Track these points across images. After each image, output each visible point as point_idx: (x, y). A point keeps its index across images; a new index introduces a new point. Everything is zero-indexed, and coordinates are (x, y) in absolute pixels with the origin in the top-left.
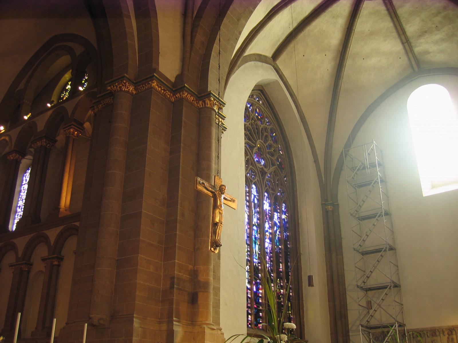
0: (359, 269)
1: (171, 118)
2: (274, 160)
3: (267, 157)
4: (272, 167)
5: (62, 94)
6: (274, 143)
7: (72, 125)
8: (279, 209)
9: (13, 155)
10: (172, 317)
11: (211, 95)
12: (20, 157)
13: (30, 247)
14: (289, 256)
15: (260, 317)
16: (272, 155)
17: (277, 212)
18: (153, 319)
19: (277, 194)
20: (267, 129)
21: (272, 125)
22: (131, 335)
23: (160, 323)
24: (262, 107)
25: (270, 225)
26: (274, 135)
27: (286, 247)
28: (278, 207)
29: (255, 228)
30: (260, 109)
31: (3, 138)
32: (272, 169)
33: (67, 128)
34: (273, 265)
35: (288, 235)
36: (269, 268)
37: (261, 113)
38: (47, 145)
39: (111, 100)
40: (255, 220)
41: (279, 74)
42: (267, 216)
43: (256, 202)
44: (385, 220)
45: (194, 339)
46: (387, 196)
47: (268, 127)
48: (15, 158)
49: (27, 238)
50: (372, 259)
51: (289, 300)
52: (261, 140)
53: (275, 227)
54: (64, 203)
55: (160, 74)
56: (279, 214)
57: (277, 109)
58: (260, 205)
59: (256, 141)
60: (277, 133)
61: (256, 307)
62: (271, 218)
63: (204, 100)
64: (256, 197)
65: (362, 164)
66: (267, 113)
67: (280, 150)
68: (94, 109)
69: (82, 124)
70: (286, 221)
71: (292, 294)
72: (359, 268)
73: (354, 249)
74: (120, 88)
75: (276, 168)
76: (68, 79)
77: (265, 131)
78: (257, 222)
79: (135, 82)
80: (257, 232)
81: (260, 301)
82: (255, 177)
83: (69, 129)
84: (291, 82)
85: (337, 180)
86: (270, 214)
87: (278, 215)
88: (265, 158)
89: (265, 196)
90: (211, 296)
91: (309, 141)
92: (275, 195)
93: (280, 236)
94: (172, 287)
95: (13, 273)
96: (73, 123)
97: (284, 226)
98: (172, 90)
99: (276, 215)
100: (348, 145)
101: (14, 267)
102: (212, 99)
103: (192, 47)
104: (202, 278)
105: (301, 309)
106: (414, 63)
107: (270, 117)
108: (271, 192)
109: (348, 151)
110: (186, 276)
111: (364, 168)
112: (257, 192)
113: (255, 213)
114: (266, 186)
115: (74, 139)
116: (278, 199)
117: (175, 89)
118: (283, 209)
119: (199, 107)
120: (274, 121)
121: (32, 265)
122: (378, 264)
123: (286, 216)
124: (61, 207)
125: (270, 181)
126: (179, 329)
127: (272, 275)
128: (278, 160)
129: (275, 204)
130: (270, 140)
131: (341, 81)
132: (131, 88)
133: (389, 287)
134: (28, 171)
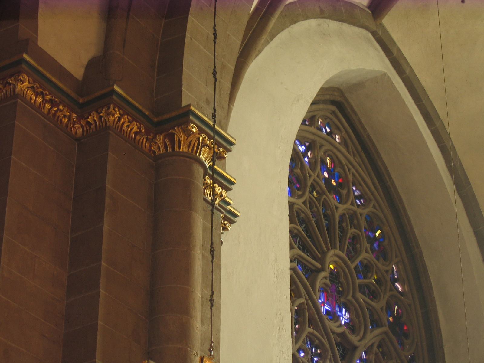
3: (357, 300)
4: (371, 332)
6: (378, 259)
11: (191, 118)
16: (373, 295)
21: (371, 205)
26: (377, 234)
37: (338, 169)
47: (359, 211)
52: (338, 252)
59: (324, 254)
67: (396, 280)
75: (386, 333)
77: (352, 223)
119: (154, 152)
128: (389, 309)
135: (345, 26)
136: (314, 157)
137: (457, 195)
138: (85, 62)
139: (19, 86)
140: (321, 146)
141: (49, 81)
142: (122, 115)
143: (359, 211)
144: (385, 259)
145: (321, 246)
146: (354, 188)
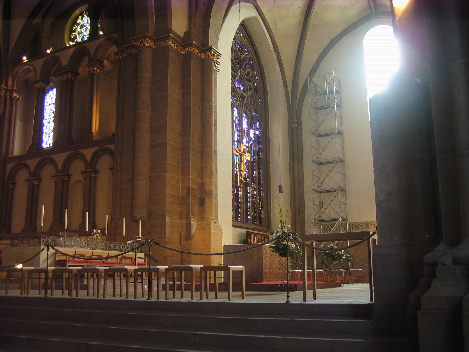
0: (316, 176)
1: (182, 68)
2: (251, 86)
3: (246, 83)
4: (249, 92)
5: (73, 27)
6: (251, 71)
7: (96, 64)
8: (254, 127)
9: (40, 84)
10: (189, 215)
11: (212, 49)
12: (46, 85)
13: (68, 162)
14: (261, 165)
15: (240, 213)
16: (250, 81)
17: (253, 129)
18: (177, 216)
19: (253, 115)
20: (246, 58)
21: (250, 54)
22: (165, 227)
23: (181, 219)
24: (243, 40)
25: (247, 140)
26: (251, 63)
27: (259, 157)
28: (253, 125)
29: (236, 143)
30: (241, 41)
31: (26, 67)
32: (250, 93)
33: (91, 66)
34: (249, 172)
35: (260, 148)
36: (246, 175)
37: (242, 45)
38: (72, 78)
39: (133, 51)
40: (236, 137)
41: (259, 11)
42: (245, 133)
43: (237, 122)
44: (338, 139)
45: (203, 229)
46: (341, 118)
47: (247, 57)
48: (42, 86)
49: (65, 155)
50: (325, 169)
51: (260, 199)
52: (241, 70)
53: (251, 142)
54: (95, 129)
55: (174, 33)
56: (254, 131)
57: (255, 40)
58: (240, 124)
59: (237, 71)
60: (254, 61)
61: (236, 205)
62: (248, 135)
63: (206, 52)
64: (237, 118)
65: (323, 91)
66: (247, 44)
67: (256, 76)
68: (118, 55)
69: (102, 62)
70: (259, 136)
71: (263, 195)
72: (315, 175)
73: (312, 161)
74: (144, 44)
75: (253, 92)
76: (78, 14)
77: (245, 60)
78: (238, 139)
79: (154, 39)
80: (237, 147)
81: (239, 200)
82: (236, 102)
83: (93, 67)
84: (267, 17)
85: (301, 101)
86: (247, 131)
87: (253, 131)
88: (244, 84)
89: (243, 116)
90: (214, 200)
91: (280, 68)
92: (252, 115)
93: (254, 149)
94: (188, 195)
95: (55, 182)
96: (96, 62)
97: (258, 140)
98: (182, 45)
99: (252, 132)
100: (312, 74)
101: (55, 177)
102: (213, 53)
103: (196, 7)
104: (207, 188)
105: (269, 206)
106: (372, 5)
107: (249, 48)
108: (248, 113)
109: (311, 79)
110: (197, 187)
111: (324, 94)
112: (238, 114)
113: (236, 131)
114: (245, 108)
115: (97, 75)
116: (254, 119)
117: (185, 44)
118: (257, 126)
119: (202, 58)
120: (252, 51)
121: (70, 176)
122: (330, 173)
123: (259, 132)
124: (93, 132)
125: (247, 104)
126: (194, 223)
127: (248, 180)
128: (254, 84)
129: (251, 123)
130: (249, 69)
131: (310, 18)
132: (152, 44)
133: (337, 191)
134: (47, 94)
135: (246, 3)
136: (235, 41)
137: (274, 51)
138: (184, 33)
139: (169, 42)
140: (237, 38)
141: (176, 40)
142: (194, 49)
143: (247, 57)
144: (253, 70)
145: (237, 69)
146: (246, 49)
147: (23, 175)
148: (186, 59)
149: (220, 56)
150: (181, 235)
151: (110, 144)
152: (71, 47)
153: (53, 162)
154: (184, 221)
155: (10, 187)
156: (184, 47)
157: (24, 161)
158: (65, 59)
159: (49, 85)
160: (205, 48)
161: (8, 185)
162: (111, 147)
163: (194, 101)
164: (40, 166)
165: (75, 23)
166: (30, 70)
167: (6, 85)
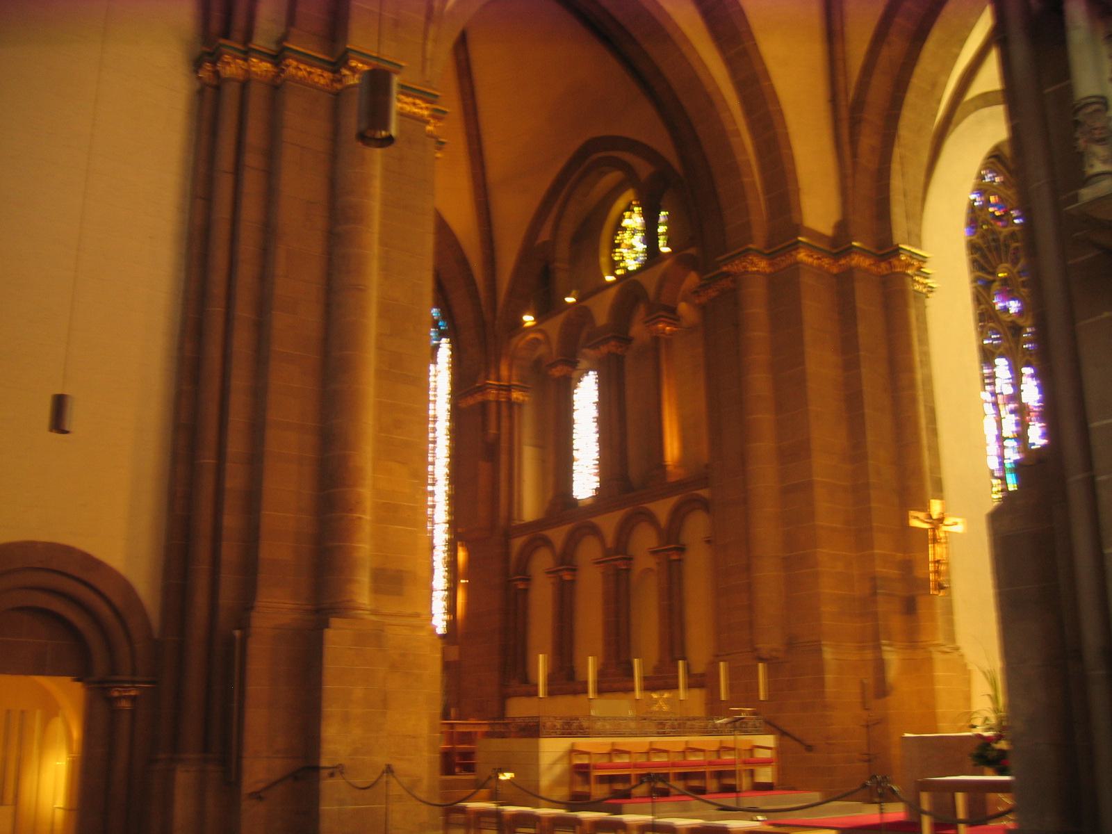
13: (625, 530)
31: (532, 336)
69: (673, 310)
74: (745, 267)
83: (654, 324)
94: (875, 594)
110: (894, 572)
126: (893, 657)
147: (542, 562)
148: (843, 284)
149: (924, 262)
150: (863, 685)
151: (702, 488)
152: (611, 284)
153: (595, 531)
154: (869, 655)
155: (521, 587)
156: (836, 256)
157: (540, 532)
158: (601, 309)
159: (579, 368)
160: (886, 251)
161: (515, 583)
162: (704, 493)
163: (871, 376)
164: (573, 541)
165: (618, 228)
166: (537, 339)
167: (498, 379)
